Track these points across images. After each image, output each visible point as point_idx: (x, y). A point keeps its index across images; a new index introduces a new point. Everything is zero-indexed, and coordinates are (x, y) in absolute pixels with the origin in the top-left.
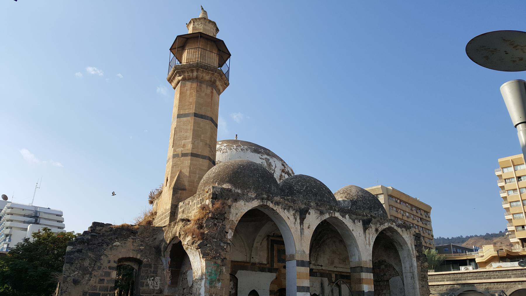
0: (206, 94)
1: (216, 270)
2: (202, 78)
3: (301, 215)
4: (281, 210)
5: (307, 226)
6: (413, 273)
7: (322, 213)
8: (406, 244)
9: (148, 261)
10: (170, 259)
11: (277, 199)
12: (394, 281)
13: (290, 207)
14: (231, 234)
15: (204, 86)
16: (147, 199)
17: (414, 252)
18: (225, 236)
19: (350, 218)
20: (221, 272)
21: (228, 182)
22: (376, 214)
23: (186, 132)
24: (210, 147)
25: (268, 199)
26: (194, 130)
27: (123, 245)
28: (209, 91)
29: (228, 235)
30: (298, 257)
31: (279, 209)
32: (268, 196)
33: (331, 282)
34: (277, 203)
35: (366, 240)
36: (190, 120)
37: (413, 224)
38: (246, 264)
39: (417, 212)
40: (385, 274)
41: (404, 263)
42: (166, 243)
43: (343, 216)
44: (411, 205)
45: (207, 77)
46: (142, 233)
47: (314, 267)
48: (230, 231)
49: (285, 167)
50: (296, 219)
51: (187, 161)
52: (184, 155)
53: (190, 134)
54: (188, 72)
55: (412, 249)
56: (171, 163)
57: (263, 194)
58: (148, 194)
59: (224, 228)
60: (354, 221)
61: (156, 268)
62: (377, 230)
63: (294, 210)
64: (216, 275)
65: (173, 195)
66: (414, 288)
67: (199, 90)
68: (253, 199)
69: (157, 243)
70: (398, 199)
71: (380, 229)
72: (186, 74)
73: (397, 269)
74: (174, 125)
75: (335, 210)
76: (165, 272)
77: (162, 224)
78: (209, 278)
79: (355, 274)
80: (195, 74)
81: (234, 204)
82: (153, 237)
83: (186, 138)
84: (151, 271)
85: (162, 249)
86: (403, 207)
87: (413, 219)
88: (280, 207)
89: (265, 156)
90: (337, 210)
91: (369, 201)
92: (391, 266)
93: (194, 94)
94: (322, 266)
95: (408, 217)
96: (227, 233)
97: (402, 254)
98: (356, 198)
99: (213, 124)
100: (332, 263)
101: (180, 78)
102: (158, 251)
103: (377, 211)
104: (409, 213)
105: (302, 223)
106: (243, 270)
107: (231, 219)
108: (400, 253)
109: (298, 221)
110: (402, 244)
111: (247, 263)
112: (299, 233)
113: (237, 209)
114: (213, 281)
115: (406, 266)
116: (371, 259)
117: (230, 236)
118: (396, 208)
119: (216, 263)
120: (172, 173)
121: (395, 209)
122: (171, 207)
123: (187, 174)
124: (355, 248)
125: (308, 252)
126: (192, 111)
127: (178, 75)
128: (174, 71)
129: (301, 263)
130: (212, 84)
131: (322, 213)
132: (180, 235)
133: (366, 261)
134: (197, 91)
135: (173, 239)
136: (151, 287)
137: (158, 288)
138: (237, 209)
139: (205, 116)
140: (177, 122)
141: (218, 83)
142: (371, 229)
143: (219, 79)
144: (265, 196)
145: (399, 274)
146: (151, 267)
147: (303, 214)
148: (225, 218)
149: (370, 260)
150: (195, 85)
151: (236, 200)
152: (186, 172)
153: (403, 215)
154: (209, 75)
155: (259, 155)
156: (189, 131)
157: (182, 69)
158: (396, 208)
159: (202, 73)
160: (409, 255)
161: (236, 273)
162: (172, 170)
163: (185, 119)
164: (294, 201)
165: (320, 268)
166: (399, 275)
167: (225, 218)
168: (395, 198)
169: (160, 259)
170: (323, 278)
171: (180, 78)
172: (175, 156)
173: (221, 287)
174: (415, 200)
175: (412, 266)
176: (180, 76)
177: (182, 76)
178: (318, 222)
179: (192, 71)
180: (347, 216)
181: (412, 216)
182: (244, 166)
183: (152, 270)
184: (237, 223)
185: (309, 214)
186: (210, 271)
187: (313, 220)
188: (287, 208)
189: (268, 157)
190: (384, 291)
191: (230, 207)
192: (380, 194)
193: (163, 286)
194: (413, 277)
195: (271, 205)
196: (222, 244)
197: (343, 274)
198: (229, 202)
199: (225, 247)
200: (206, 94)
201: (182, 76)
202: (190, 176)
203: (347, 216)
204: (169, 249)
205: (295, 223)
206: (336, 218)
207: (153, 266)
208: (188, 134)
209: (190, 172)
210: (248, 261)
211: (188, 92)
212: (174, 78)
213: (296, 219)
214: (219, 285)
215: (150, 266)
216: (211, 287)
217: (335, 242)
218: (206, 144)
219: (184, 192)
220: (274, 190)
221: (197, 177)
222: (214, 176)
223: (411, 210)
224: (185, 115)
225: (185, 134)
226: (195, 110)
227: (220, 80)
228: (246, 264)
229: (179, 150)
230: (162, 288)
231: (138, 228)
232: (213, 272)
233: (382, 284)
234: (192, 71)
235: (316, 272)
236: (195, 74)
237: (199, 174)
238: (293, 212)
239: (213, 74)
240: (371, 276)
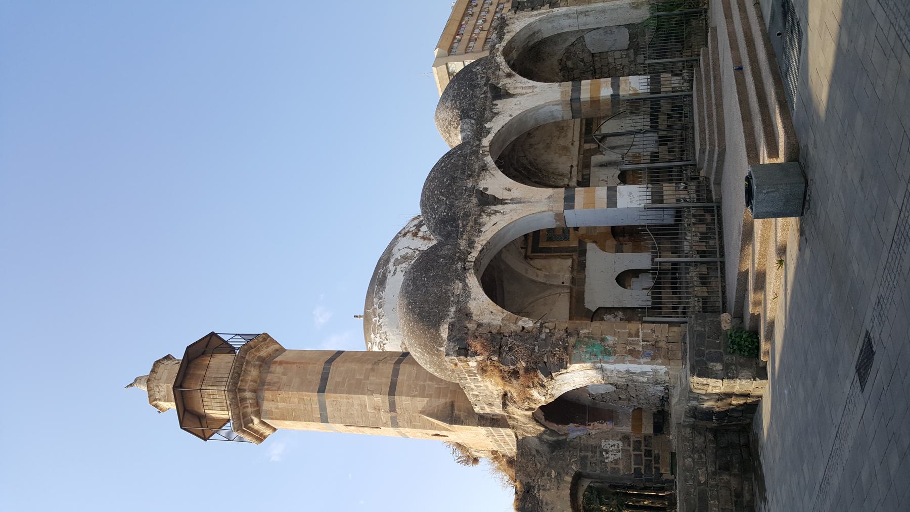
0: (284, 374)
1: (587, 344)
2: (255, 382)
3: (489, 204)
4: (482, 238)
5: (506, 193)
6: (579, 13)
7: (484, 168)
8: (530, 25)
9: (575, 462)
10: (571, 425)
11: (463, 244)
12: (593, 44)
13: (476, 222)
14: (524, 321)
15: (269, 378)
16: (471, 468)
17: (543, 11)
18: (529, 332)
19: (490, 120)
20: (589, 337)
21: (437, 330)
22: (482, 77)
23: (352, 405)
24: (377, 363)
25: (464, 260)
26: (349, 392)
27: (549, 507)
28: (278, 369)
29: (526, 326)
30: (559, 206)
31: (481, 241)
32: (459, 259)
33: (598, 151)
34: (471, 244)
35: (526, 93)
36: (330, 398)
37: (496, 12)
39: (476, 6)
40: (583, 60)
41: (562, 29)
42: (544, 432)
43: (488, 132)
44: (465, 14)
45: (254, 373)
46: (528, 475)
47: (574, 180)
48: (521, 323)
49: (409, 232)
50: (496, 212)
51: (402, 401)
52: (392, 407)
53: (356, 399)
54: (244, 408)
55: (540, 14)
56: (407, 431)
57: (456, 268)
58: (462, 466)
59: (516, 334)
60: (496, 114)
61: (586, 448)
62: (509, 75)
63: (480, 215)
64: (593, 345)
65: (462, 423)
66: (603, 11)
67: (278, 387)
68: (466, 285)
69: (544, 449)
70: (454, 38)
71: (508, 70)
72: (249, 410)
73: (573, 39)
74: (340, 427)
75: (478, 146)
76: (594, 432)
77: (512, 441)
78: (600, 357)
79: (583, 111)
80: (248, 395)
81: (475, 318)
82: (534, 456)
83: (363, 406)
84: (592, 457)
85: (555, 438)
86: (467, 29)
87: (488, 12)
88: (477, 239)
89: (391, 266)
90: (477, 142)
91: (460, 89)
92: (568, 50)
93: (283, 394)
94: (572, 166)
95: (485, 21)
96: (523, 328)
97: (547, 31)
98: (456, 111)
99: (338, 359)
100: (566, 149)
101: (256, 421)
102: (557, 445)
103: (476, 74)
104: (477, 20)
105: (502, 202)
106: (584, 299)
107: (499, 323)
108: (546, 35)
109: (499, 207)
110: (531, 33)
111: (571, 292)
112: (520, 206)
113: (482, 313)
114: (605, 350)
115: (567, 25)
116: (557, 84)
117: (528, 323)
118: (469, 41)
119: (574, 346)
120: (424, 428)
121: (472, 44)
122: (484, 425)
123: (426, 400)
124: (541, 111)
125: (549, 191)
126: (315, 396)
127: (251, 425)
128: (244, 432)
129: (569, 201)
130: (265, 363)
131: (484, 168)
132: (530, 409)
133: (562, 92)
134: (279, 389)
135: (537, 421)
136: (620, 455)
137: (621, 443)
138: (482, 313)
139: (323, 374)
140: (335, 422)
141: (263, 353)
142: (508, 86)
143: (256, 351)
144: (459, 265)
145: (580, 35)
146: (586, 457)
147: (487, 200)
148: (499, 333)
150: (268, 394)
151: (468, 315)
152: (421, 403)
153: (482, 30)
154: (249, 369)
155: (389, 276)
156: (350, 401)
157: (239, 418)
158: (469, 41)
159: (246, 382)
160: (549, 19)
162: (420, 428)
163: (329, 409)
164: (466, 216)
165: (575, 169)
166: (583, 37)
167: (499, 333)
168: (453, 43)
169: (571, 441)
170: (592, 164)
171: (256, 421)
172: (395, 424)
173: (614, 335)
174: (455, 9)
175: (567, 15)
176: (252, 421)
177: (253, 417)
178: (499, 174)
179: (243, 400)
180: (488, 125)
181: (483, 14)
182: (410, 303)
183: (590, 454)
184: (506, 312)
185: (486, 189)
186: (588, 356)
187: (496, 182)
188: (478, 227)
189: (392, 261)
190: (611, 60)
191: (480, 325)
192: (448, 68)
193: (617, 435)
194: (586, 13)
195: (475, 254)
196: (543, 336)
197: (584, 130)
198: (471, 326)
199: (547, 331)
200: (284, 374)
201: (253, 417)
202: (430, 396)
203: (488, 125)
204: (554, 427)
205: (503, 213)
206: (492, 144)
207: (583, 454)
208: (356, 402)
209: (422, 395)
211: (281, 405)
212: (256, 431)
213: (496, 212)
214: (611, 340)
215: (583, 459)
216: (615, 353)
217: (531, 145)
218: (373, 370)
219: (456, 404)
220: (449, 250)
221: (430, 383)
222: (429, 353)
223: (472, 15)
224: (323, 408)
225: (356, 407)
226: (312, 391)
227: (258, 350)
229: (385, 416)
230: (620, 436)
231: (521, 482)
232: (590, 350)
233: (598, 65)
234: (243, 400)
235: (583, 175)
236: (248, 395)
237: (425, 381)
238: (484, 216)
239: (248, 362)
240: (586, 84)
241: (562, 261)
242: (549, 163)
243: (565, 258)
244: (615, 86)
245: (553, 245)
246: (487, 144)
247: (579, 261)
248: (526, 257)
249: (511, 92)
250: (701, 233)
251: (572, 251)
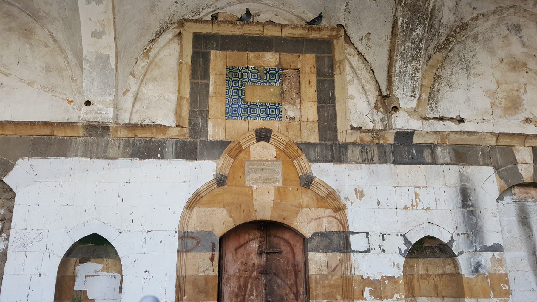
33: (512, 183)
38: (59, 133)
47: (414, 124)
94: (461, 121)
100: (514, 105)
106: (44, 155)
161: (8, 168)
170: (468, 170)
210: (74, 119)
217: (517, 28)
228: (59, 133)
235: (432, 147)
241: (172, 105)
242: (467, 68)
243: (178, 114)
245: (216, 82)
247: (161, 144)
248: (182, 22)
251: (192, 125)
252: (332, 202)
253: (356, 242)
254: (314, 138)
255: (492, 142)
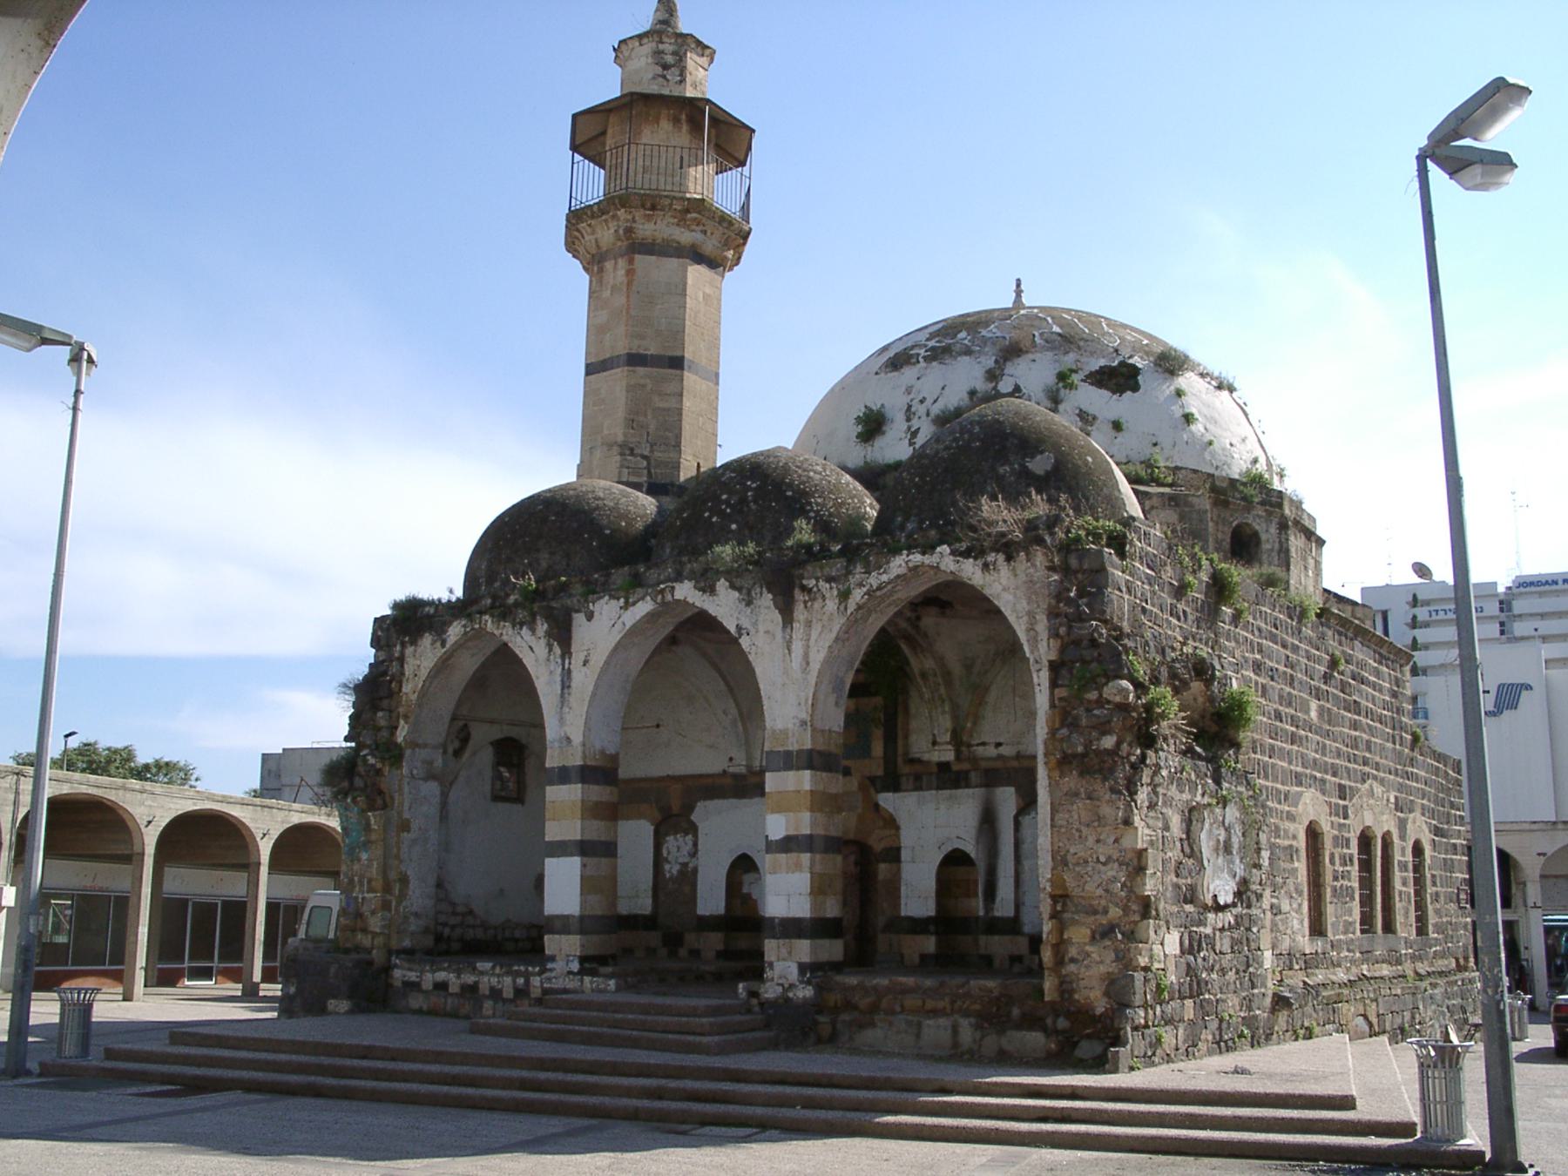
17: (1043, 646)
19: (733, 587)
43: (710, 589)
99: (641, 370)
109: (557, 650)
149: (803, 723)
159: (593, 233)
161: (691, 808)
244: (788, 844)
246: (679, 595)
249: (800, 613)
250: (500, 991)
252: (892, 823)
253: (904, 855)
254: (880, 772)
255: (1015, 764)
